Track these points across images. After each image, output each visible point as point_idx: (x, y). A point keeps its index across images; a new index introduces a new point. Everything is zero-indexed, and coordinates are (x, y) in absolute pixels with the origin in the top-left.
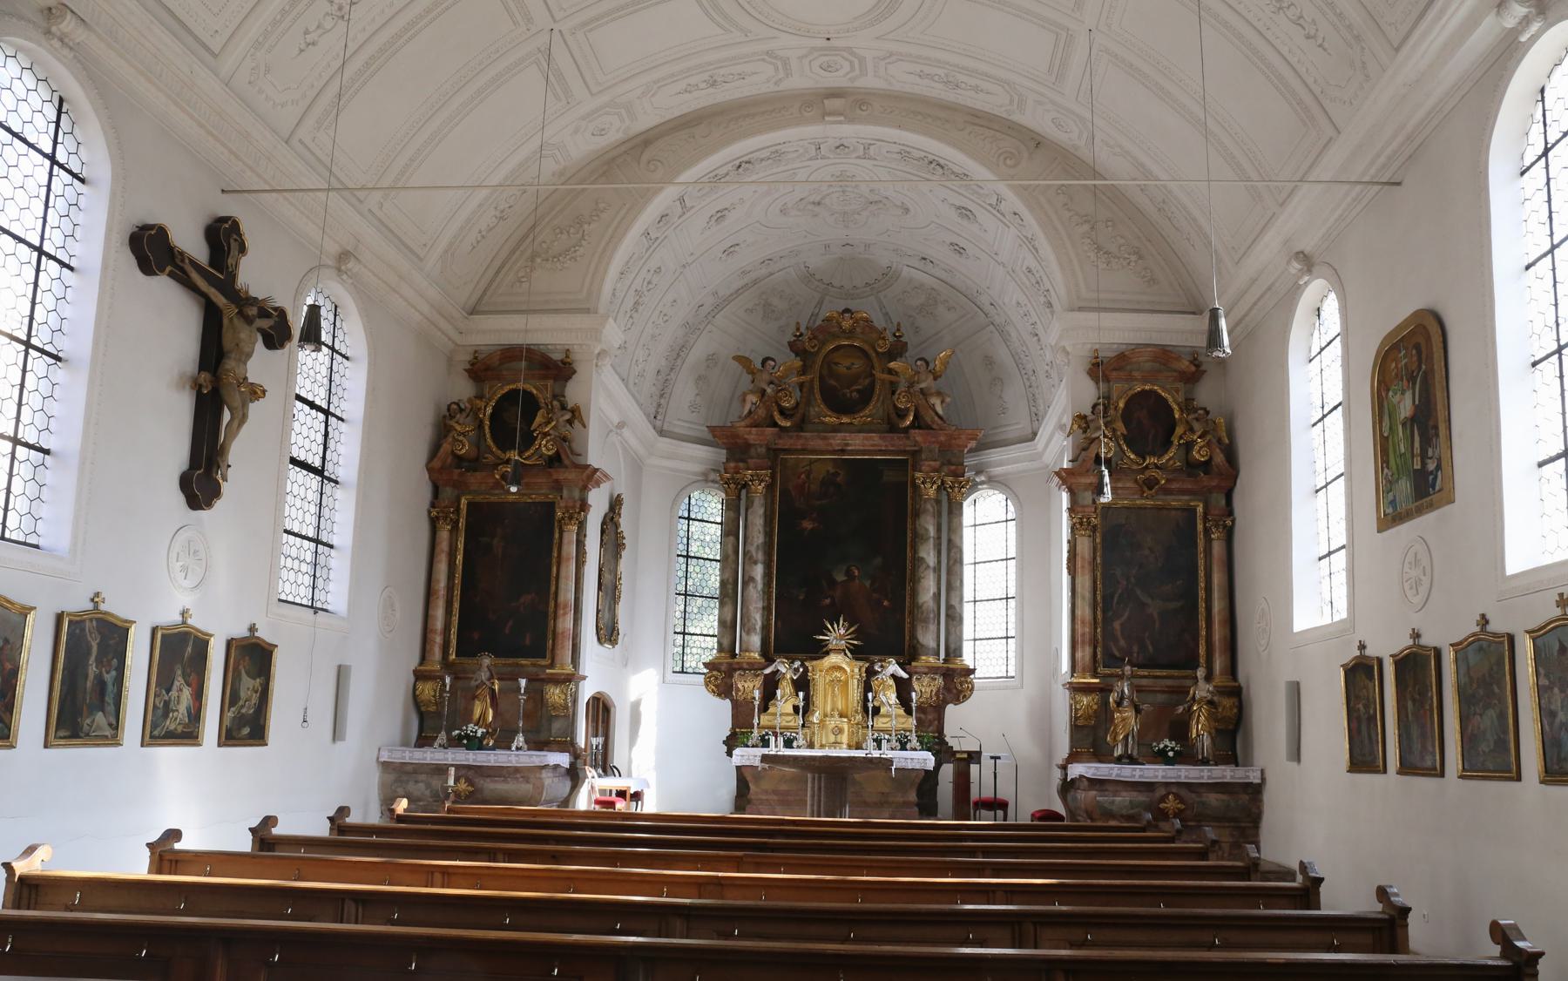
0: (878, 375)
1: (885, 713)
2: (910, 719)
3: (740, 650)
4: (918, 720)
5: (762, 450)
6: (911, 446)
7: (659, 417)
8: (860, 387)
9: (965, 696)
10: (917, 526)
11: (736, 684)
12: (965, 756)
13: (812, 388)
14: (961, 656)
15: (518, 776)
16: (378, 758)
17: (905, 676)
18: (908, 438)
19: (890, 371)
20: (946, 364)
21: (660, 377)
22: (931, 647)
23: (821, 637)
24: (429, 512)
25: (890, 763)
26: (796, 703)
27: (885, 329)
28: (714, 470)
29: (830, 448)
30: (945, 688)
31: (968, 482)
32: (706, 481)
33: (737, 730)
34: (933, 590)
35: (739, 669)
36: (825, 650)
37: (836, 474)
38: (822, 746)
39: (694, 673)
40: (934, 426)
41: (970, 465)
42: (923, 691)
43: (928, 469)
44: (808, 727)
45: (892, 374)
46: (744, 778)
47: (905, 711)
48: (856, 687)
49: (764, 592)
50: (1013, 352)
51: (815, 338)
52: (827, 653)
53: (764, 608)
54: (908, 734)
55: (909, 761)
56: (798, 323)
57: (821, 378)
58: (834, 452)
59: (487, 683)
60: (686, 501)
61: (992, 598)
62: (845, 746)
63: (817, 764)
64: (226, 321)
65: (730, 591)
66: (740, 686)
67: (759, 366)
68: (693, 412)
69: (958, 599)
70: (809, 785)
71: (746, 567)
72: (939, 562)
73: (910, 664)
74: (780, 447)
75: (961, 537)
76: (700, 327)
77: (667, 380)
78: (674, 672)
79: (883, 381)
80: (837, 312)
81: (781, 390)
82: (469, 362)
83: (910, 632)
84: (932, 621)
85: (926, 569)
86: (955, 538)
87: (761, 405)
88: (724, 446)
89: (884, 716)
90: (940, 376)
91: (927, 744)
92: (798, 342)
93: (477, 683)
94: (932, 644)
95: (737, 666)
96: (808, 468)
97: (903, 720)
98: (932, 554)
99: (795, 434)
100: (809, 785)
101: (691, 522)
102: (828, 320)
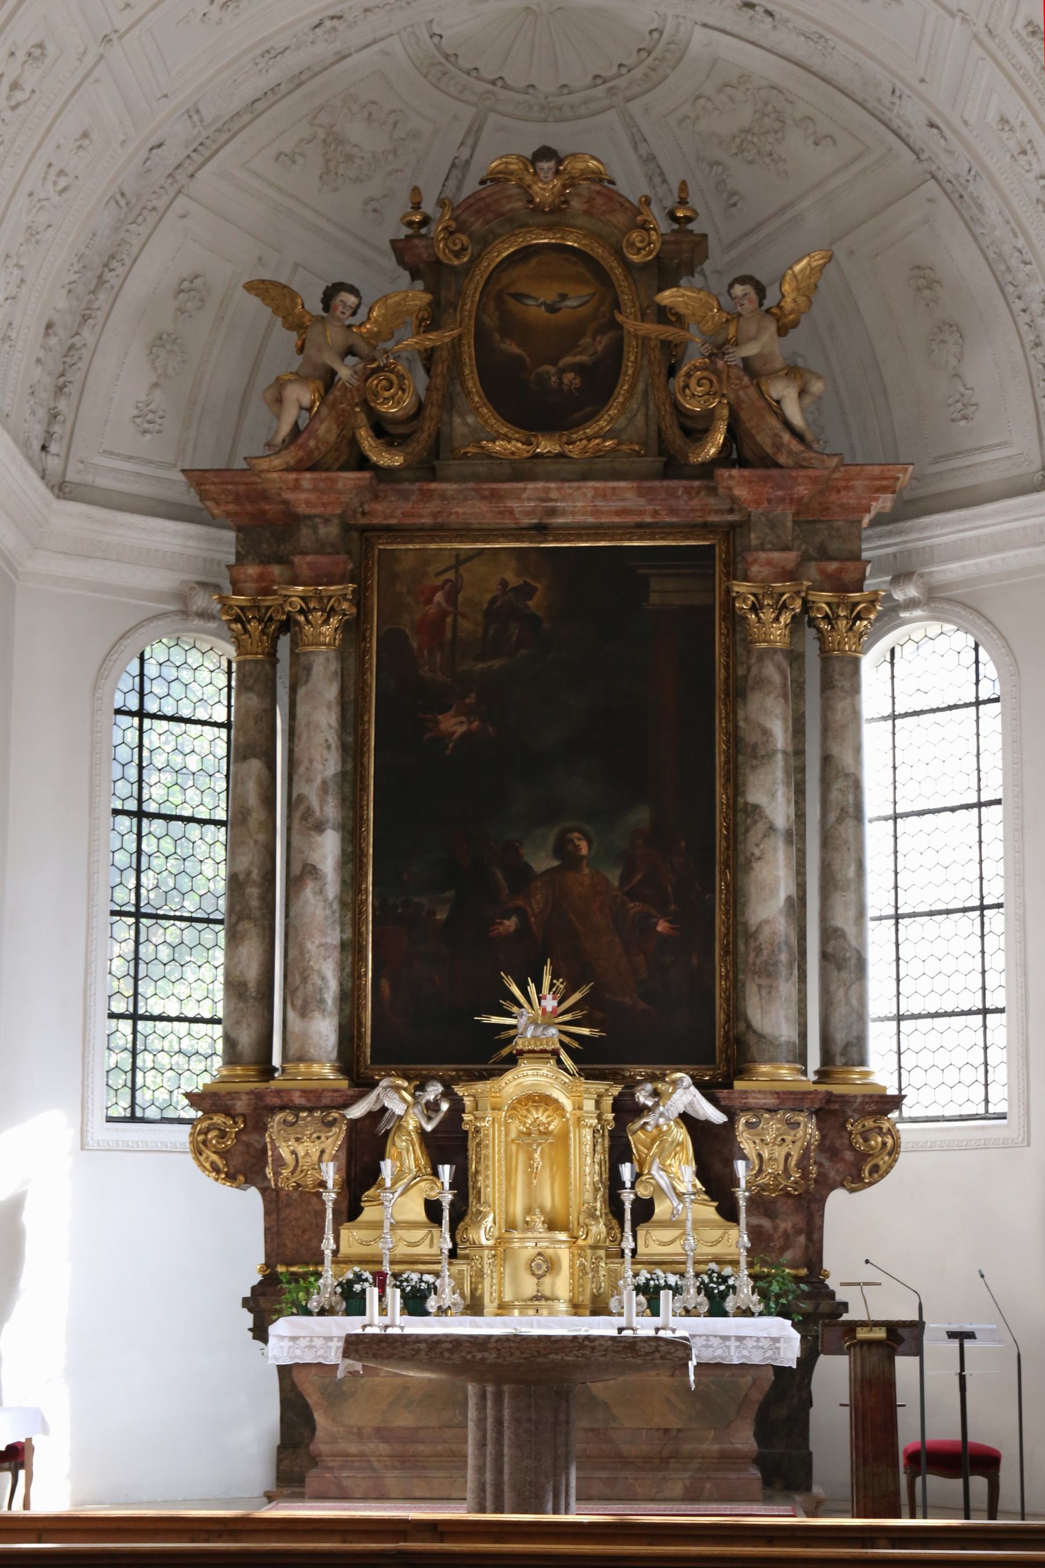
0: (631, 324)
1: (667, 1217)
2: (733, 1233)
3: (285, 1058)
4: (755, 1233)
5: (330, 531)
6: (718, 512)
7: (53, 448)
8: (578, 359)
9: (875, 1169)
10: (741, 724)
11: (275, 1148)
12: (881, 1334)
13: (456, 360)
14: (862, 1063)
17: (717, 1117)
18: (713, 491)
19: (664, 315)
20: (809, 290)
21: (53, 341)
22: (783, 1039)
23: (495, 1020)
25: (680, 1354)
26: (433, 1195)
27: (648, 201)
28: (203, 585)
29: (508, 522)
30: (821, 1147)
31: (873, 602)
32: (185, 613)
33: (281, 1269)
34: (785, 889)
35: (282, 1108)
36: (505, 1052)
37: (525, 591)
38: (503, 1308)
39: (164, 1120)
40: (782, 459)
41: (873, 557)
42: (766, 1155)
43: (766, 571)
44: (466, 1257)
45: (669, 323)
46: (301, 1396)
47: (718, 1209)
48: (588, 1148)
49: (343, 904)
50: (991, 254)
51: (462, 228)
52: (512, 1061)
53: (343, 946)
54: (727, 1270)
55: (733, 1344)
56: (416, 190)
57: (481, 335)
58: (518, 532)
60: (134, 667)
61: (943, 907)
62: (562, 1306)
63: (491, 1357)
65: (255, 903)
66: (285, 1152)
67: (315, 306)
68: (145, 432)
69: (852, 913)
70: (472, 1413)
71: (296, 840)
72: (800, 816)
73: (730, 1086)
74: (376, 521)
75: (858, 749)
76: (155, 203)
77: (72, 347)
78: (110, 1120)
79: (645, 340)
80: (519, 157)
81: (375, 371)
83: (727, 1000)
84: (784, 972)
85: (765, 836)
86: (842, 753)
87: (325, 411)
88: (229, 522)
89: (664, 1224)
90: (795, 324)
91: (778, 1296)
92: (416, 241)
94: (786, 1032)
95: (276, 1101)
96: (450, 575)
97: (716, 1234)
98: (780, 794)
99: (416, 486)
100: (472, 1413)
101: (147, 723)
102: (494, 179)
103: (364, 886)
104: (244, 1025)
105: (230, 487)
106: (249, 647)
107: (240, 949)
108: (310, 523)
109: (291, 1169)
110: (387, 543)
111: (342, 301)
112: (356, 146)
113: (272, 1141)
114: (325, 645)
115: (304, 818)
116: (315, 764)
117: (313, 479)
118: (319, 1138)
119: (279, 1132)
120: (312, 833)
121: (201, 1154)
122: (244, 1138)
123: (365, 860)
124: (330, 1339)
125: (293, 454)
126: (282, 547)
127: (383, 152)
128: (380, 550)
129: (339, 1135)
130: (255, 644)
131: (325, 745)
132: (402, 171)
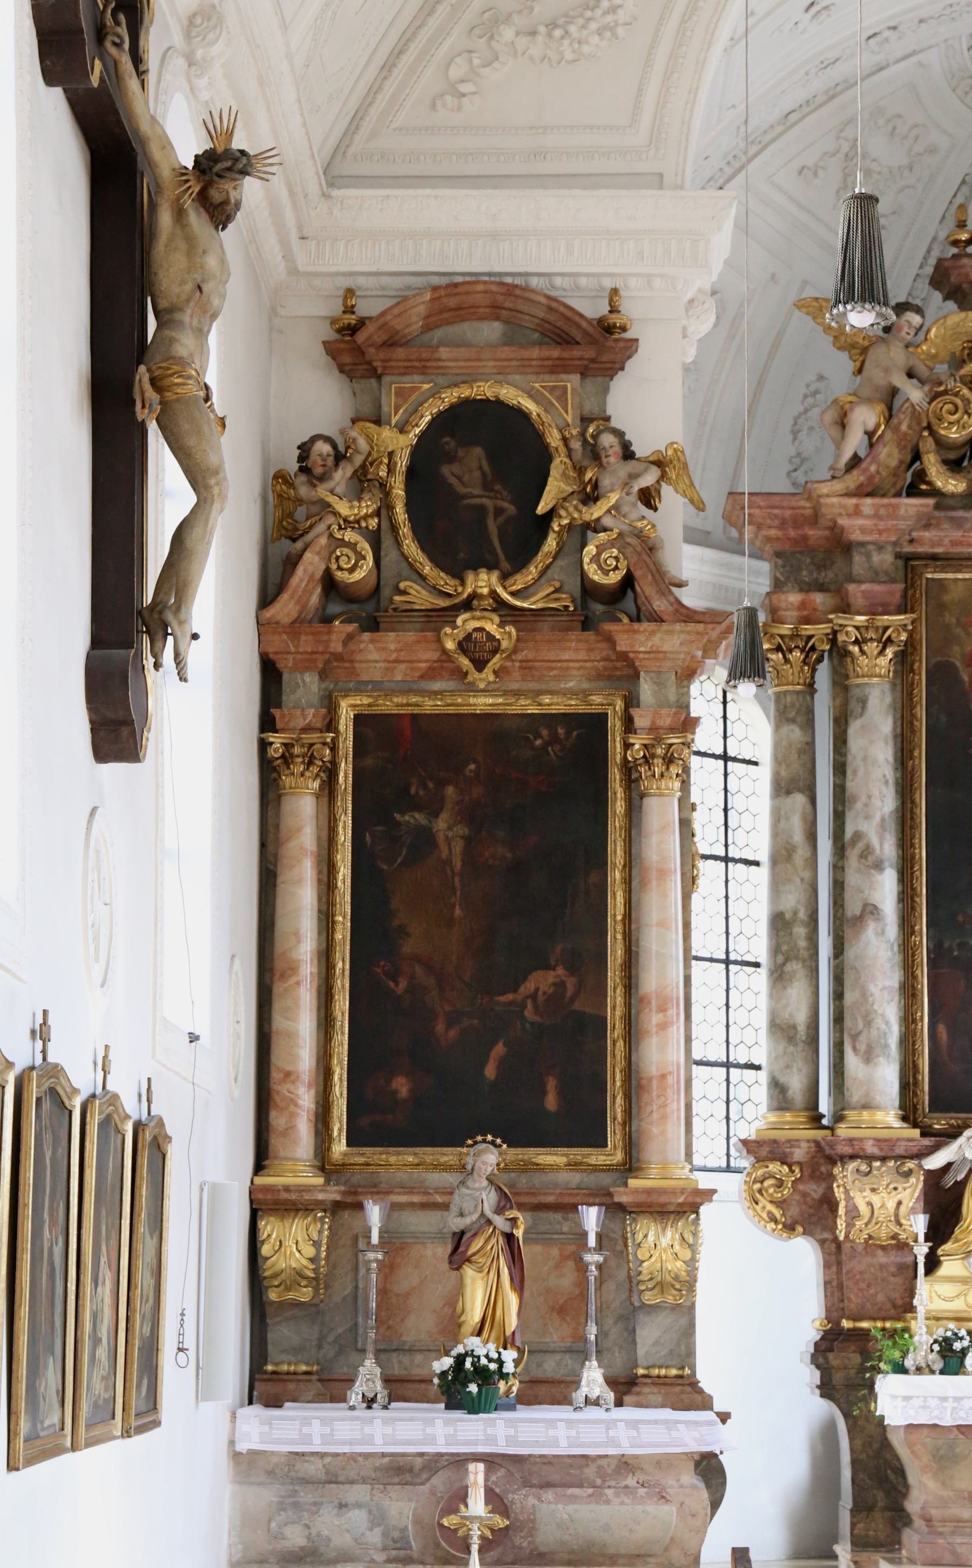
5: (884, 559)
11: (849, 1199)
15: (631, 1481)
16: (232, 1443)
24: (263, 746)
35: (853, 1157)
59: (499, 1221)
64: (165, 218)
65: (802, 943)
74: (920, 549)
82: (333, 321)
87: (889, 435)
92: (965, 261)
93: (468, 1221)
95: (847, 1150)
103: (917, 928)
104: (795, 1070)
105: (776, 511)
106: (791, 678)
107: (789, 990)
108: (863, 550)
109: (866, 1220)
110: (935, 572)
111: (908, 322)
112: (874, 160)
113: (847, 1192)
114: (880, 676)
115: (864, 855)
116: (873, 800)
117: (873, 505)
118: (895, 1189)
119: (854, 1182)
120: (872, 871)
121: (757, 1203)
122: (801, 1187)
123: (917, 900)
124: (945, 1399)
125: (855, 478)
126: (823, 574)
127: (900, 167)
128: (927, 579)
129: (916, 1186)
130: (796, 674)
131: (883, 780)
132: (914, 187)
